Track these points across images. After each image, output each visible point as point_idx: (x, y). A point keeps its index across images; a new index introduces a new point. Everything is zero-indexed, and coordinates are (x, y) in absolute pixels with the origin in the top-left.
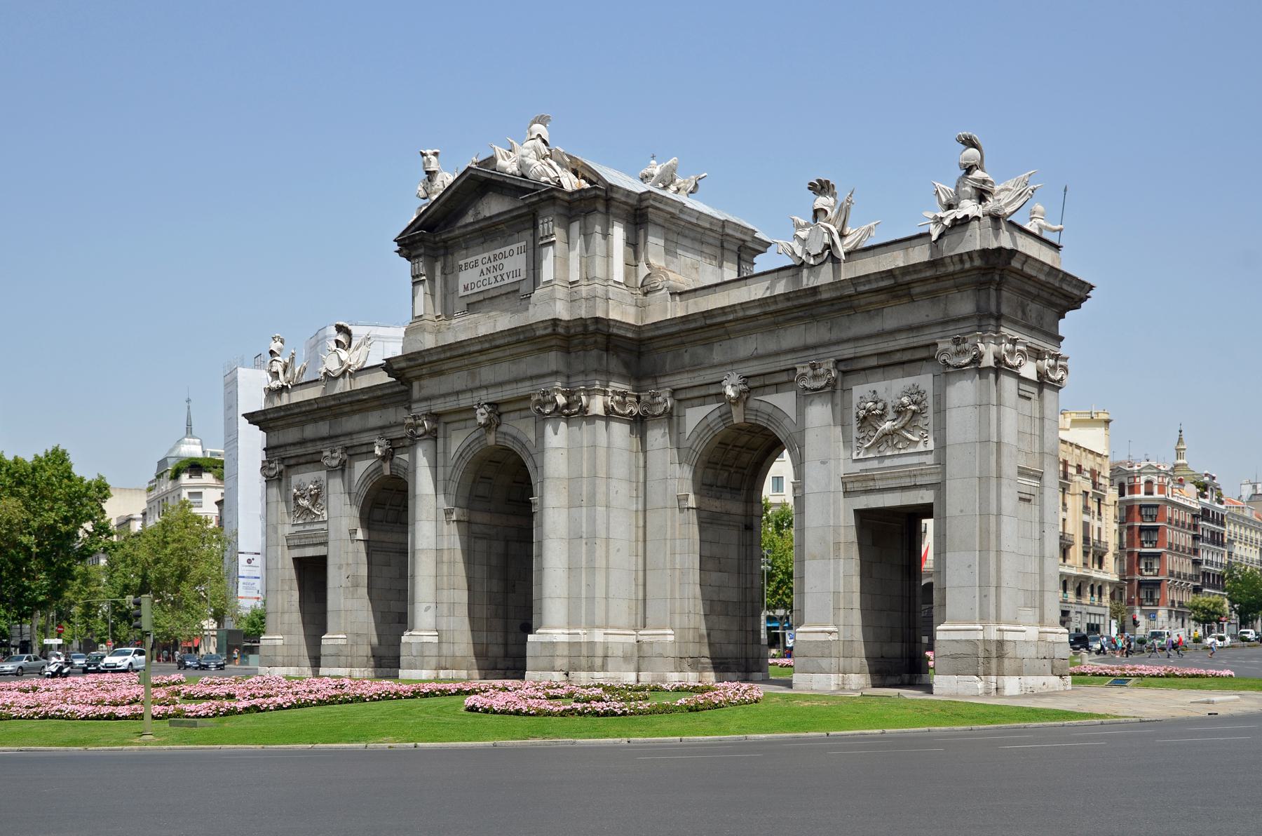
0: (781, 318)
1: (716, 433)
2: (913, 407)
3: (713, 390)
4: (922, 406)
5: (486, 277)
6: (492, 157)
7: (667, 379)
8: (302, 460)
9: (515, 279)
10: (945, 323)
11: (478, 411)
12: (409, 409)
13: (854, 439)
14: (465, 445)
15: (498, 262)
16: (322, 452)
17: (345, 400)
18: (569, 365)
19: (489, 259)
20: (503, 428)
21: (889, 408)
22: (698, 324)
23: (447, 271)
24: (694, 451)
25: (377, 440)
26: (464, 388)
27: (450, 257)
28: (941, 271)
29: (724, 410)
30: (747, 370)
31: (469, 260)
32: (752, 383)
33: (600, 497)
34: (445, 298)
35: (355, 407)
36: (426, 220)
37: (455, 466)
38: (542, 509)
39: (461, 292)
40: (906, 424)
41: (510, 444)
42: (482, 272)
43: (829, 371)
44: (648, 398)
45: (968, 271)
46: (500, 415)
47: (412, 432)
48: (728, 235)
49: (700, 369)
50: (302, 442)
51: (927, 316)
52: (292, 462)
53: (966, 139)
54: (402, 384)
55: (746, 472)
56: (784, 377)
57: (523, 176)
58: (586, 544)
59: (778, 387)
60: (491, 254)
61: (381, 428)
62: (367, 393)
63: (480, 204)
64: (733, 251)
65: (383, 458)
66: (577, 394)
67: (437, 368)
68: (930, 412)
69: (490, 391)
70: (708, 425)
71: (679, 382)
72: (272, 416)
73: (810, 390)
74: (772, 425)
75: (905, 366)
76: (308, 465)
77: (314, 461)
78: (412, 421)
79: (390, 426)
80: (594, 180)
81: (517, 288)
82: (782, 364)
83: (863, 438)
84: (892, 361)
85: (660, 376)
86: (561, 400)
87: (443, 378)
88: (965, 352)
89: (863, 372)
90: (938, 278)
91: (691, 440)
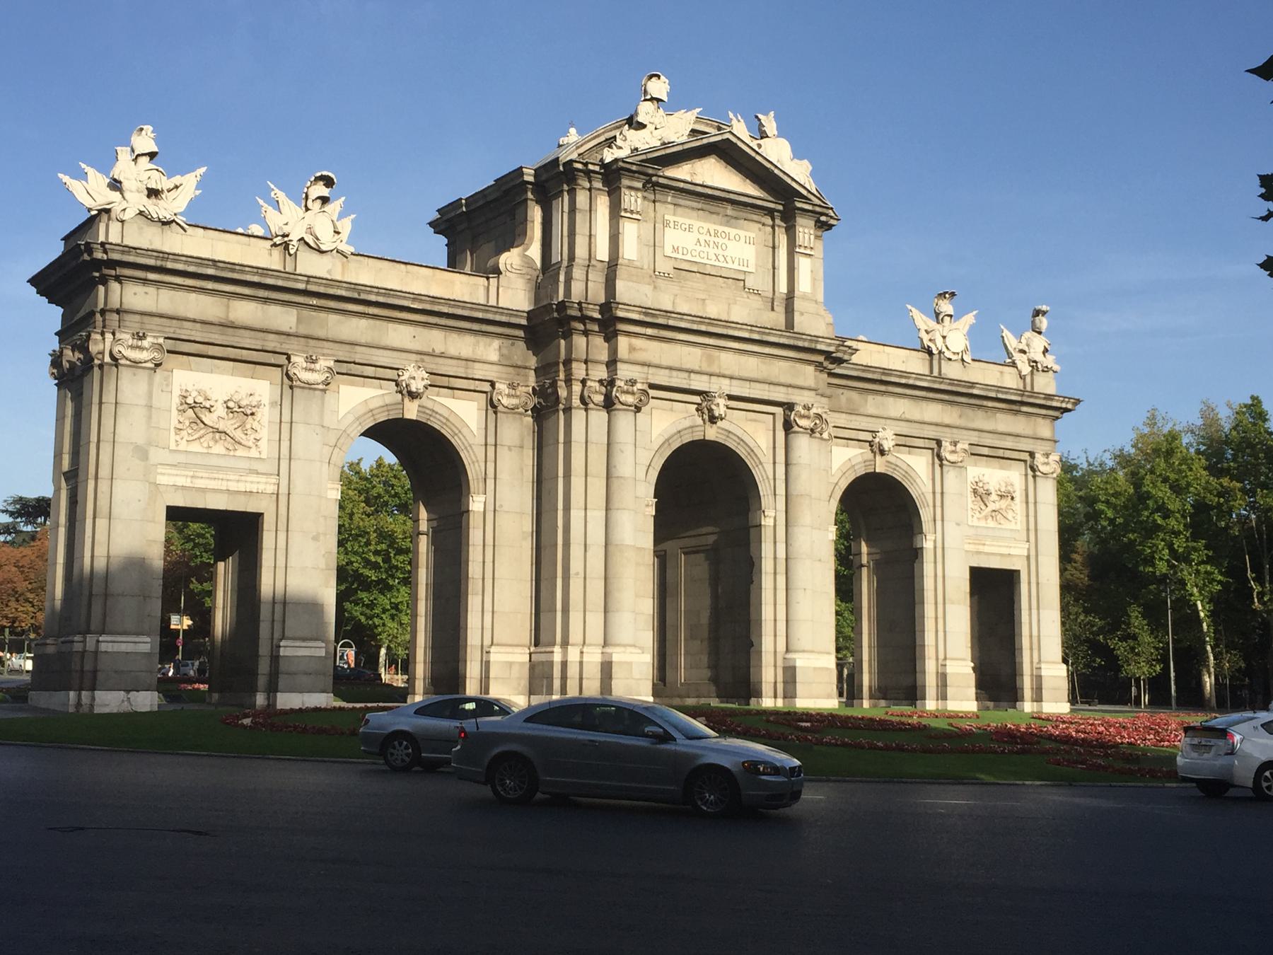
0: (931, 395)
9: (741, 268)
15: (720, 241)
25: (411, 369)
26: (697, 368)
31: (680, 220)
39: (668, 252)
41: (731, 444)
60: (712, 227)
62: (421, 301)
65: (413, 395)
69: (734, 382)
79: (432, 355)
82: (925, 432)
88: (1047, 464)
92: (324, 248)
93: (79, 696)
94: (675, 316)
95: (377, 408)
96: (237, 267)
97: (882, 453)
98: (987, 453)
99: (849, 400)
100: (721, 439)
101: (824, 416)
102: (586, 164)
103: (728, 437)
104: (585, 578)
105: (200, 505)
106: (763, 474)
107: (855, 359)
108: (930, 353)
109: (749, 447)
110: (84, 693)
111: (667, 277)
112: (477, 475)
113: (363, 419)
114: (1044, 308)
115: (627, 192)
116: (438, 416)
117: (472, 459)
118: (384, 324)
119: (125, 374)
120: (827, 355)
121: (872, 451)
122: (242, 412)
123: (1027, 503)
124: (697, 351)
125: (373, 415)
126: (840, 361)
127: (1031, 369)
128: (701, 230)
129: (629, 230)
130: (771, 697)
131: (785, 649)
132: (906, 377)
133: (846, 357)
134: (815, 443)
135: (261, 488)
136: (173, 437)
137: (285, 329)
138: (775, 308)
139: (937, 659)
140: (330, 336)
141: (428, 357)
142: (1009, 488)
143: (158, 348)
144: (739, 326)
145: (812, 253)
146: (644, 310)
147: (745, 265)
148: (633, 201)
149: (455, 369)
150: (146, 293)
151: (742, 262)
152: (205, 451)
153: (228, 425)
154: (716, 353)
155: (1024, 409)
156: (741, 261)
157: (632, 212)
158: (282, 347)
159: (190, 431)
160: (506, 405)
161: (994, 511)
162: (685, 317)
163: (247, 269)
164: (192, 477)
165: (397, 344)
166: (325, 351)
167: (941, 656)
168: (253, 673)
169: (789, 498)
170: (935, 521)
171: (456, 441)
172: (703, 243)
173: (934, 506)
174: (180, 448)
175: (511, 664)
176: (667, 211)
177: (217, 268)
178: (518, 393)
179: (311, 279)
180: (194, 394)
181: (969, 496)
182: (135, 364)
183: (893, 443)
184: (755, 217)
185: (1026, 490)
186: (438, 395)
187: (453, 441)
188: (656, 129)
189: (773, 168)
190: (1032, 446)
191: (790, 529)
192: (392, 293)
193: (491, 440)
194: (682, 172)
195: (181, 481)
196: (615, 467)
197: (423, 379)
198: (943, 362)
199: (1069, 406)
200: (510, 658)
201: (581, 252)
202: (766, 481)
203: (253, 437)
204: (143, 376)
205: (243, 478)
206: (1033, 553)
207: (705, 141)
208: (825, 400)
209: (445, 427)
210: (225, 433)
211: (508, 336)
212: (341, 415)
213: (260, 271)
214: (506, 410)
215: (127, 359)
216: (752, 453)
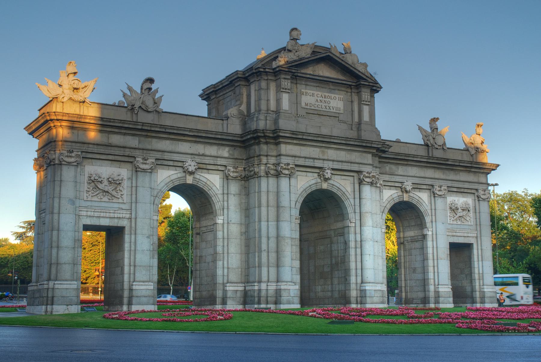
0: (429, 165)
3: (397, 184)
9: (337, 112)
15: (327, 100)
19: (322, 96)
20: (331, 182)
25: (189, 162)
26: (317, 157)
30: (414, 181)
31: (309, 91)
41: (335, 190)
56: (425, 187)
61: (192, 154)
62: (193, 132)
63: (316, 67)
65: (191, 173)
68: (471, 212)
69: (335, 163)
75: (463, 193)
81: (338, 116)
82: (427, 182)
87: (302, 148)
88: (484, 194)
92: (149, 110)
93: (47, 308)
94: (307, 134)
95: (174, 179)
96: (112, 120)
97: (407, 192)
98: (456, 191)
99: (390, 168)
101: (377, 176)
102: (265, 69)
103: (333, 187)
104: (268, 252)
105: (98, 224)
106: (350, 203)
107: (390, 150)
108: (428, 145)
109: (342, 191)
110: (48, 306)
111: (303, 117)
112: (220, 208)
113: (168, 185)
114: (481, 124)
115: (283, 80)
116: (202, 182)
117: (217, 201)
118: (177, 142)
119: (65, 168)
120: (378, 149)
121: (402, 191)
122: (115, 183)
123: (476, 212)
124: (317, 150)
125: (173, 182)
126: (384, 152)
127: (476, 151)
128: (318, 95)
129: (285, 97)
130: (355, 304)
131: (361, 282)
132: (416, 157)
133: (386, 150)
134: (374, 189)
135: (124, 215)
137: (133, 146)
138: (353, 128)
139: (435, 285)
140: (153, 148)
141: (197, 156)
142: (467, 206)
143: (77, 156)
144: (336, 138)
145: (369, 104)
146: (292, 132)
147: (339, 110)
148: (286, 84)
149: (208, 161)
150: (73, 133)
151: (337, 109)
152: (99, 200)
153: (110, 188)
154: (326, 150)
155: (473, 170)
156: (337, 108)
157: (286, 89)
158: (133, 154)
159: (93, 192)
160: (232, 176)
161: (460, 217)
162: (311, 135)
163: (116, 121)
164: (94, 212)
165: (183, 151)
166: (151, 155)
167: (436, 283)
168: (122, 297)
169: (361, 214)
170: (432, 222)
171: (210, 193)
172: (319, 101)
173: (432, 215)
174: (89, 199)
175: (237, 291)
176: (302, 88)
178: (238, 171)
179: (144, 124)
180: (94, 176)
181: (448, 210)
182: (69, 164)
183: (411, 187)
184: (343, 89)
185: (475, 207)
187: (208, 192)
188: (296, 52)
189: (350, 67)
191: (362, 228)
192: (180, 128)
193: (226, 192)
194: (309, 70)
195: (89, 213)
196: (281, 202)
197: (194, 166)
198: (434, 150)
199: (494, 168)
200: (236, 288)
201: (263, 107)
202: (351, 206)
203: (120, 193)
204: (72, 169)
205: (116, 212)
206: (479, 235)
207: (318, 57)
208: (378, 169)
209: (205, 186)
210: (108, 192)
211: (232, 146)
212: (159, 183)
213: (122, 122)
214: (232, 178)
215: (65, 161)
216: (344, 194)
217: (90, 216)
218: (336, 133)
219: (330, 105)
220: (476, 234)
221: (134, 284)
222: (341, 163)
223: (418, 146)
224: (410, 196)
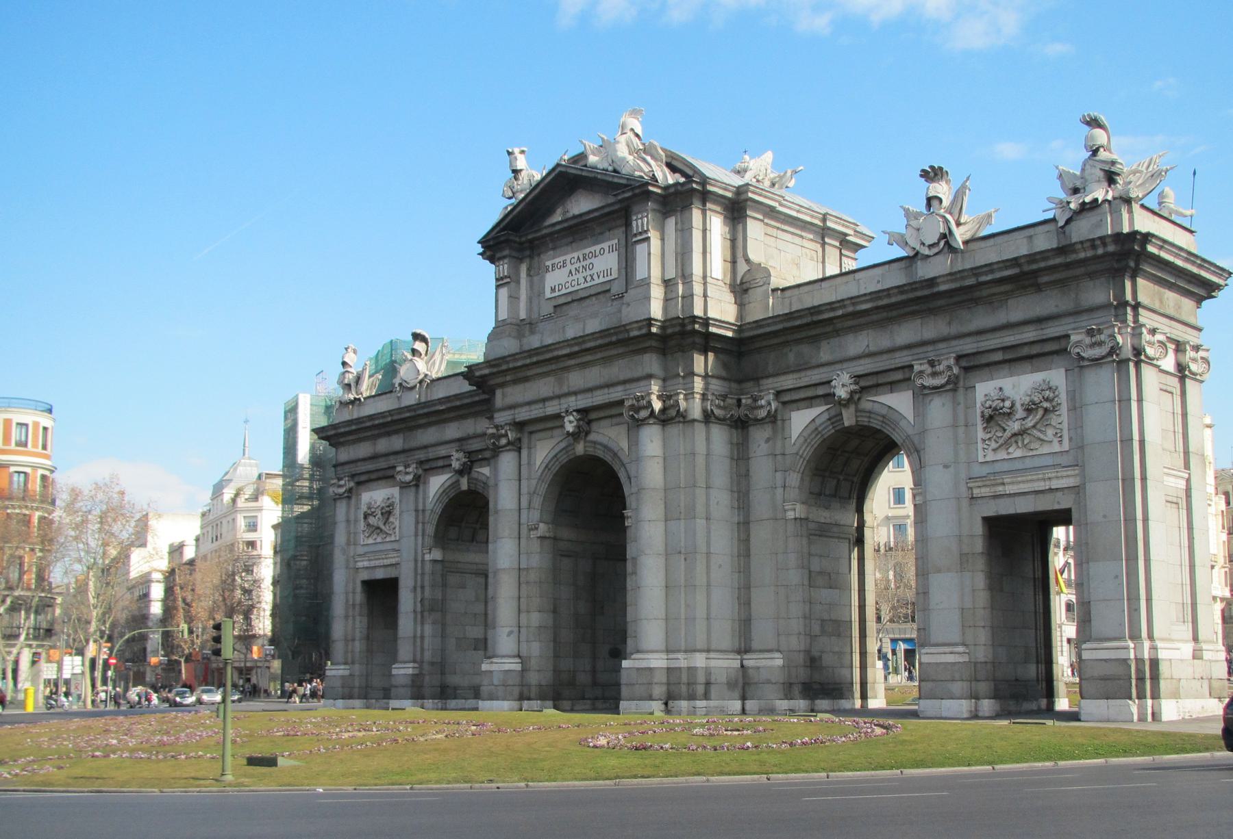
0: (894, 313)
1: (825, 436)
2: (1046, 405)
3: (821, 391)
4: (1054, 403)
5: (575, 277)
6: (583, 153)
7: (770, 380)
8: (373, 476)
10: (1077, 313)
11: (566, 419)
12: (491, 418)
13: (979, 441)
14: (551, 456)
15: (588, 261)
16: (394, 467)
17: (421, 412)
18: (665, 369)
19: (578, 258)
20: (592, 437)
21: (1018, 405)
22: (804, 321)
23: (532, 273)
24: (801, 457)
25: (454, 453)
26: (551, 394)
27: (536, 258)
28: (1073, 257)
29: (833, 413)
31: (556, 261)
32: (863, 383)
33: (700, 509)
34: (531, 302)
35: (433, 419)
36: (512, 220)
37: (539, 479)
38: (638, 521)
39: (548, 294)
40: (1037, 423)
41: (600, 453)
42: (571, 272)
43: (949, 368)
44: (749, 401)
45: (1103, 256)
46: (589, 422)
47: (494, 443)
48: (829, 229)
49: (806, 369)
50: (374, 457)
51: (1057, 306)
52: (363, 478)
53: (1091, 119)
54: (484, 392)
55: (855, 479)
56: (898, 376)
57: (615, 171)
58: (685, 559)
59: (892, 386)
60: (580, 254)
63: (568, 202)
64: (835, 247)
65: (460, 472)
66: (675, 398)
67: (520, 375)
68: (1064, 409)
69: (579, 397)
70: (816, 429)
71: (784, 383)
72: (342, 430)
73: (929, 388)
74: (887, 427)
75: (1034, 361)
76: (380, 482)
77: (386, 476)
78: (494, 431)
79: (468, 438)
80: (690, 173)
81: (608, 288)
82: (897, 361)
83: (990, 439)
84: (1019, 355)
85: (762, 378)
86: (657, 405)
87: (527, 385)
88: (1100, 344)
89: (987, 369)
90: (1067, 266)
91: (798, 445)
100: (591, 451)
105: (373, 578)
111: (549, 318)
124: (551, 379)
132: (840, 307)
134: (674, 430)
136: (362, 536)
142: (1033, 397)
145: (646, 236)
155: (1044, 279)
161: (1015, 435)
177: (356, 424)
183: (853, 387)
186: (481, 467)
190: (1073, 326)
194: (557, 217)
195: (366, 564)
210: (378, 528)
217: (367, 568)
218: (593, 326)
219: (591, 272)
220: (1078, 479)
221: (394, 666)
222: (589, 395)
223: (887, 266)
224: (861, 411)
